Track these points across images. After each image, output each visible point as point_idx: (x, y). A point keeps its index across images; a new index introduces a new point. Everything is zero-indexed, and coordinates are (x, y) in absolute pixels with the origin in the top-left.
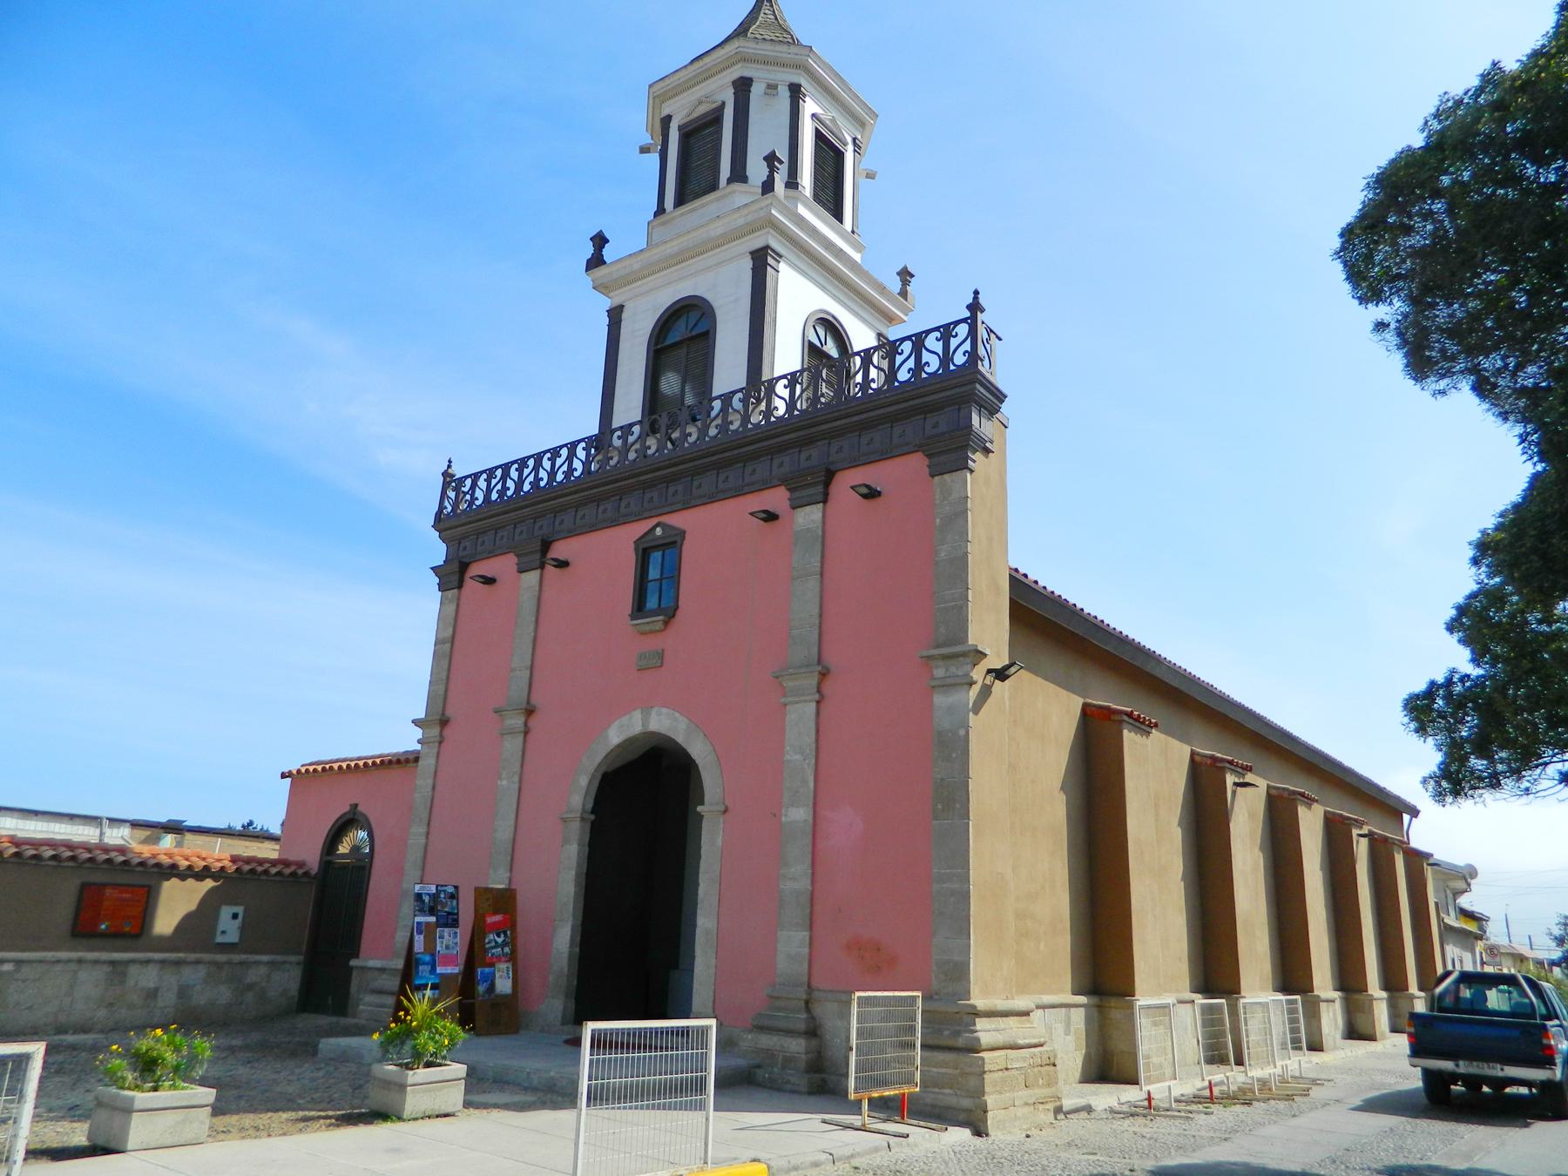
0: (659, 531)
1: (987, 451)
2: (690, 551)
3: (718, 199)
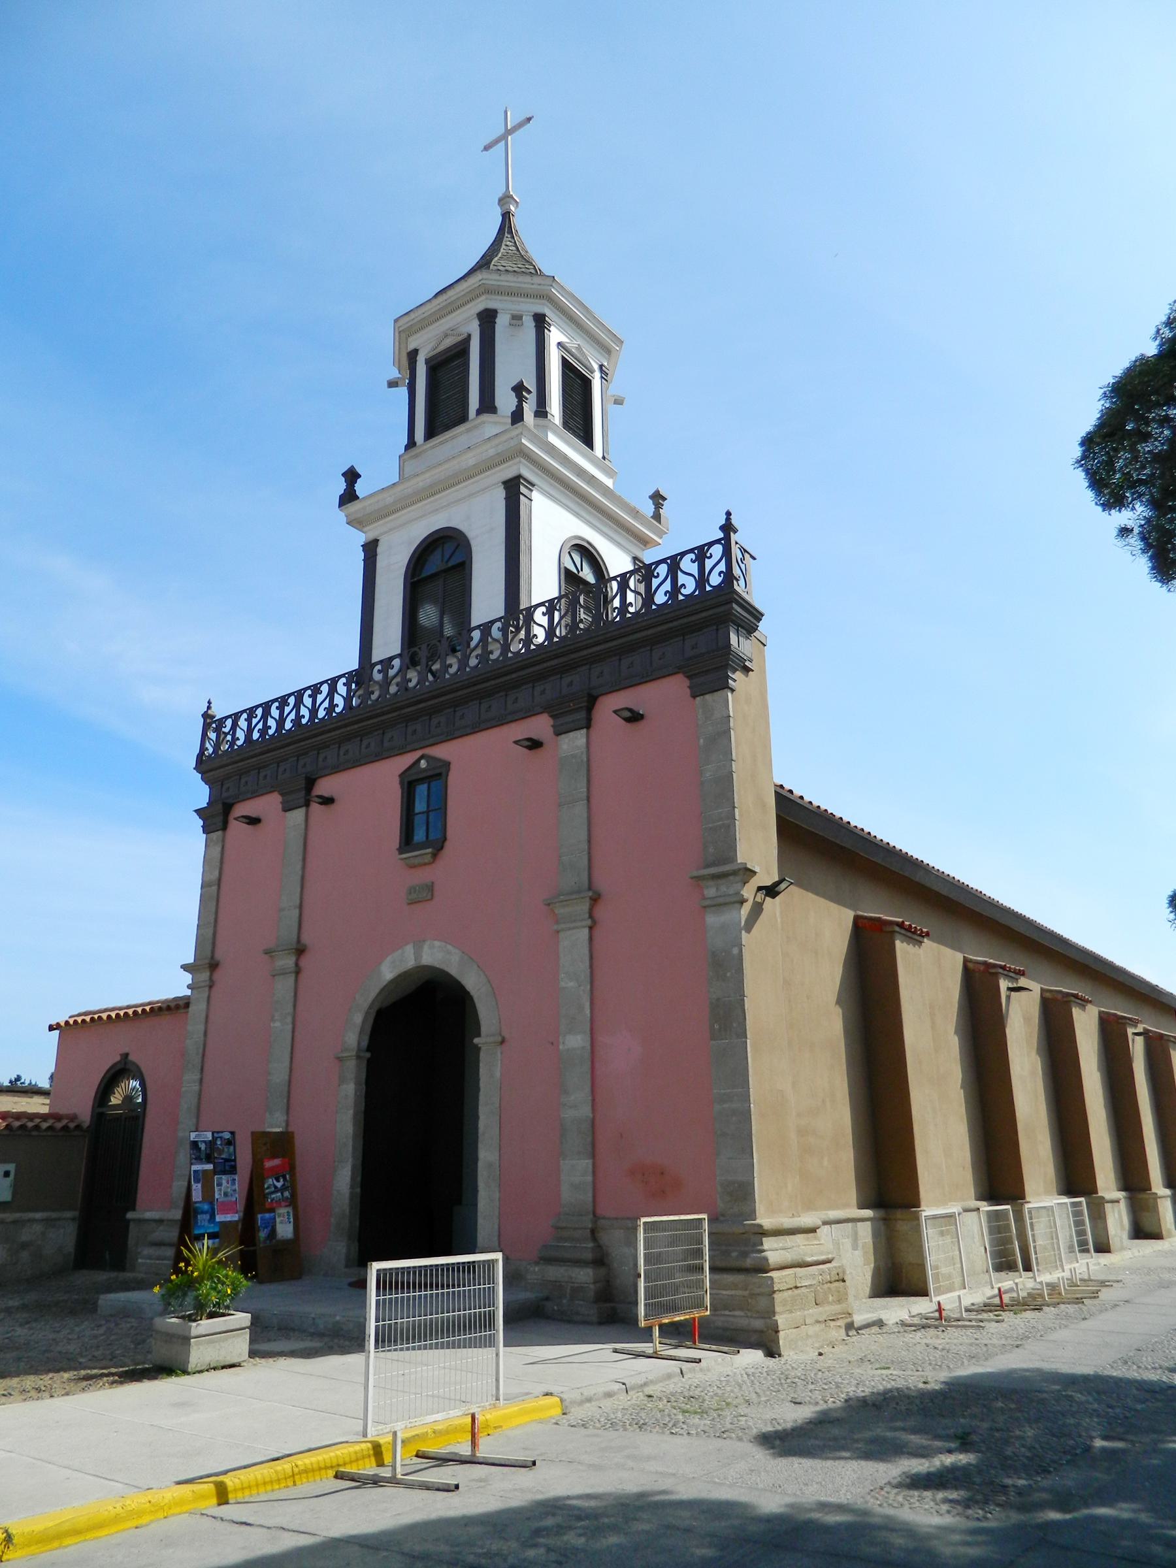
1: (747, 670)
3: (468, 430)
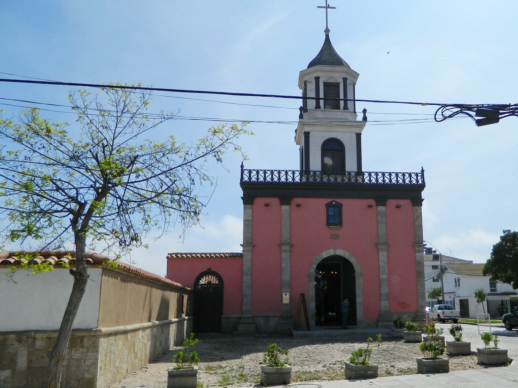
0: (334, 203)
2: (344, 209)
